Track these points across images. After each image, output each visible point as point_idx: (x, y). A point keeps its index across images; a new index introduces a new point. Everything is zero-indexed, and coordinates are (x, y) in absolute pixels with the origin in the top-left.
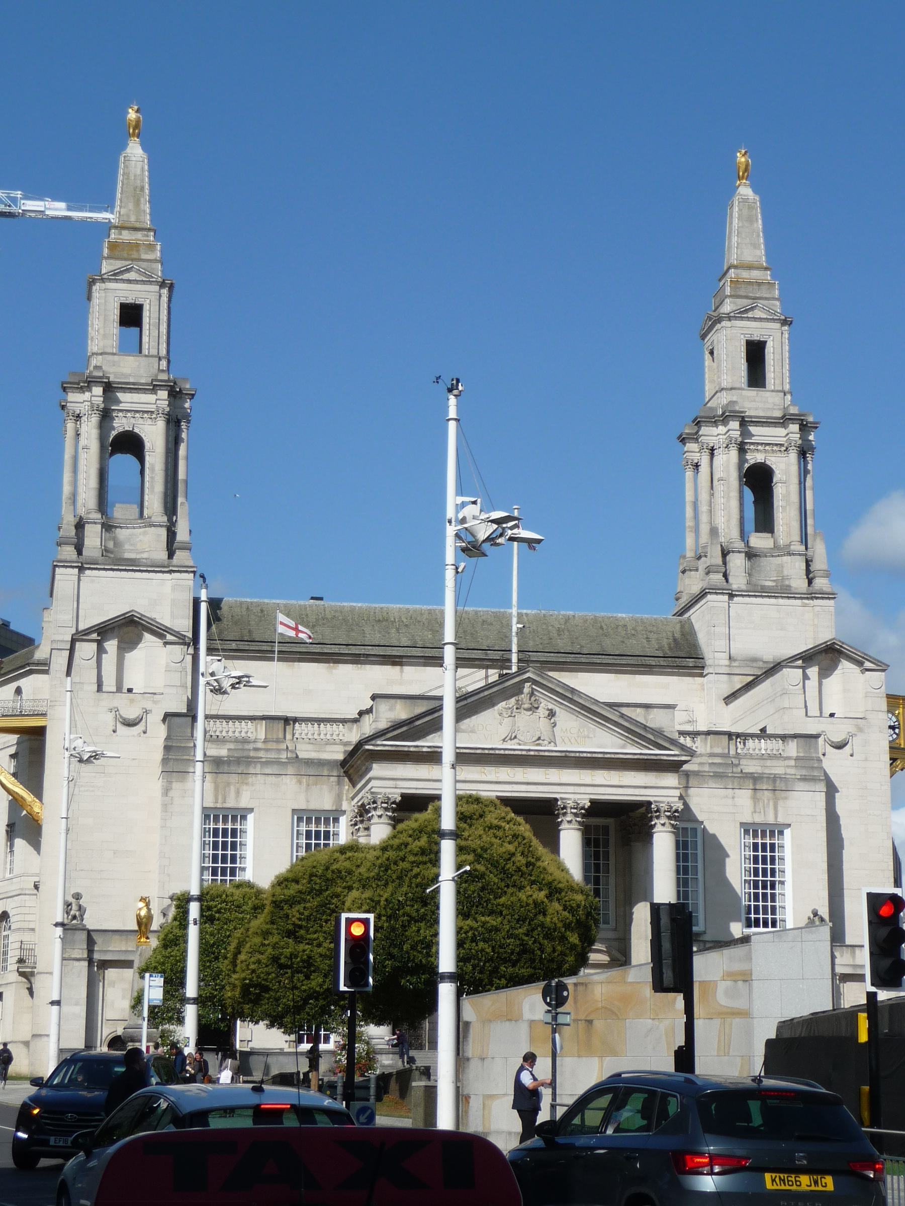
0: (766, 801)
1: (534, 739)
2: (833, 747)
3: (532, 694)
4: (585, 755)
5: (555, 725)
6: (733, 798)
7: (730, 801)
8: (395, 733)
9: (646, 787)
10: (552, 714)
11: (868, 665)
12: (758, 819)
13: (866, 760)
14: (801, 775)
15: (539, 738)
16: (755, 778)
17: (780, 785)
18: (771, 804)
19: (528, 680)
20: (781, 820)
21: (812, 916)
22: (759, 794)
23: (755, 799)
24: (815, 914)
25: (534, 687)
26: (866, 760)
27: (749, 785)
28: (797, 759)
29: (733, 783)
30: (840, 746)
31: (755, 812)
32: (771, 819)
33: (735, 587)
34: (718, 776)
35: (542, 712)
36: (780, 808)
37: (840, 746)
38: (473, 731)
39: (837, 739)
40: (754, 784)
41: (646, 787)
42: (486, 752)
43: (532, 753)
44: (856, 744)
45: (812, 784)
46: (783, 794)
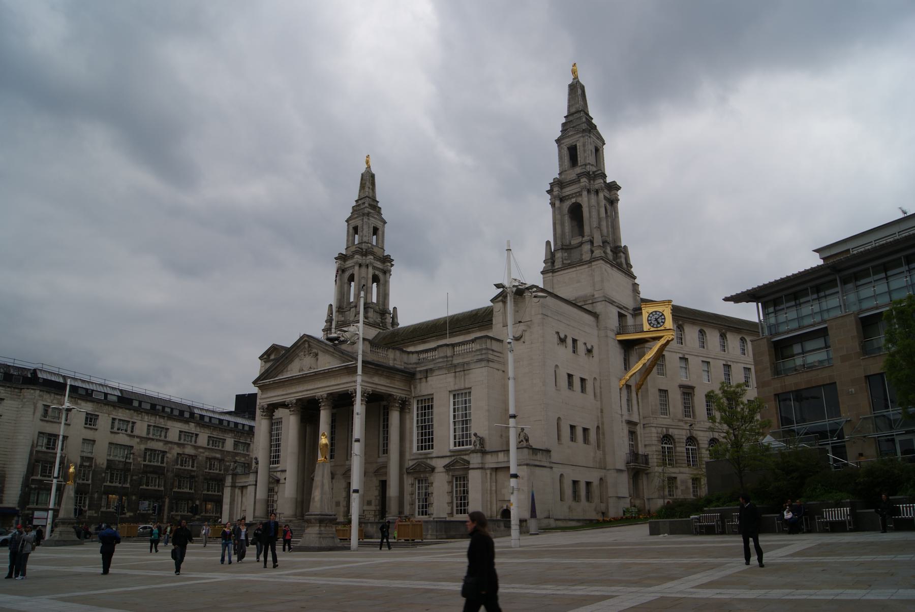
1: (308, 369)
3: (309, 346)
4: (321, 372)
5: (317, 359)
8: (263, 377)
9: (347, 383)
10: (317, 355)
12: (457, 388)
13: (532, 343)
15: (310, 368)
16: (455, 366)
17: (466, 367)
18: (463, 377)
19: (305, 341)
20: (467, 386)
22: (457, 373)
23: (455, 377)
25: (310, 343)
26: (532, 343)
28: (477, 350)
32: (462, 387)
33: (556, 267)
34: (440, 368)
35: (312, 354)
38: (292, 370)
40: (455, 369)
41: (347, 383)
42: (290, 379)
43: (304, 376)
44: (527, 337)
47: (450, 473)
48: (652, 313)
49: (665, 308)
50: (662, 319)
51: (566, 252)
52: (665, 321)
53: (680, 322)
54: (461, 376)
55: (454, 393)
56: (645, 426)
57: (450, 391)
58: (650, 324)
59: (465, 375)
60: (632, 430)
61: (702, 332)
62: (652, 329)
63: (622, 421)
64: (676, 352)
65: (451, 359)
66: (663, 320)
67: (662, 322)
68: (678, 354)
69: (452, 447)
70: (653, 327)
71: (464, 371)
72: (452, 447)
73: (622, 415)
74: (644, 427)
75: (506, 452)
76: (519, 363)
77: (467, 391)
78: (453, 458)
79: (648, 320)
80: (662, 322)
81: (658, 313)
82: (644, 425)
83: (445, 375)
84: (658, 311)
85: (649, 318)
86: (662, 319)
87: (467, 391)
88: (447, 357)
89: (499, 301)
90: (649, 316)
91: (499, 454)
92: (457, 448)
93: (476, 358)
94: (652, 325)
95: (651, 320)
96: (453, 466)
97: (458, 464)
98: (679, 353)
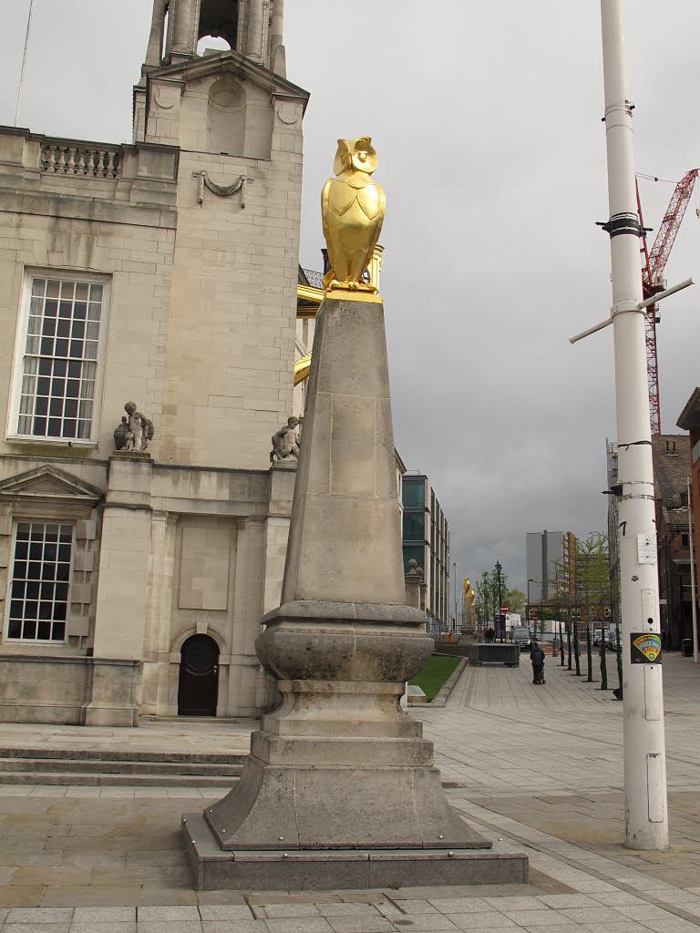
0: (74, 236)
2: (216, 193)
6: (19, 226)
7: (12, 232)
11: (279, 91)
12: (56, 261)
14: (138, 203)
16: (59, 200)
18: (83, 240)
20: (96, 265)
21: (127, 415)
22: (63, 225)
23: (54, 231)
24: (130, 409)
27: (48, 211)
29: (21, 203)
30: (224, 193)
31: (53, 250)
32: (79, 263)
36: (97, 251)
37: (224, 193)
39: (223, 182)
40: (57, 209)
44: (250, 193)
45: (156, 215)
46: (104, 228)
47: (9, 509)
54: (79, 235)
55: (40, 276)
57: (26, 267)
59: (92, 235)
65: (37, 177)
69: (12, 430)
71: (90, 221)
72: (12, 430)
75: (227, 475)
76: (220, 254)
77: (90, 281)
78: (22, 467)
83: (15, 216)
87: (90, 281)
88: (18, 166)
89: (174, 84)
91: (204, 477)
92: (32, 437)
93: (136, 198)
96: (22, 490)
97: (48, 486)
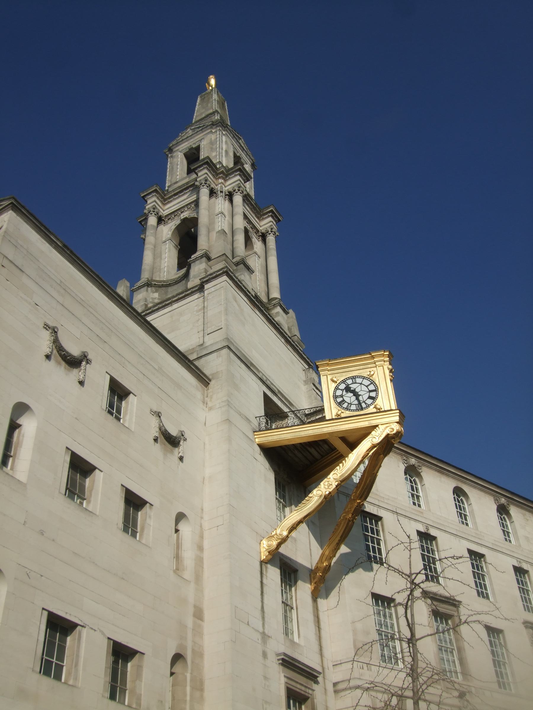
48: (344, 382)
49: (375, 369)
50: (370, 391)
51: (156, 292)
52: (377, 395)
53: (413, 461)
56: (340, 686)
58: (340, 404)
60: (298, 688)
61: (458, 492)
62: (347, 413)
63: (265, 655)
64: (410, 518)
66: (373, 394)
67: (370, 397)
68: (412, 522)
70: (347, 409)
73: (265, 637)
74: (336, 692)
79: (335, 397)
80: (370, 397)
81: (359, 380)
82: (335, 684)
84: (359, 377)
85: (339, 393)
86: (370, 391)
90: (337, 388)
94: (345, 405)
95: (342, 396)
98: (416, 520)
